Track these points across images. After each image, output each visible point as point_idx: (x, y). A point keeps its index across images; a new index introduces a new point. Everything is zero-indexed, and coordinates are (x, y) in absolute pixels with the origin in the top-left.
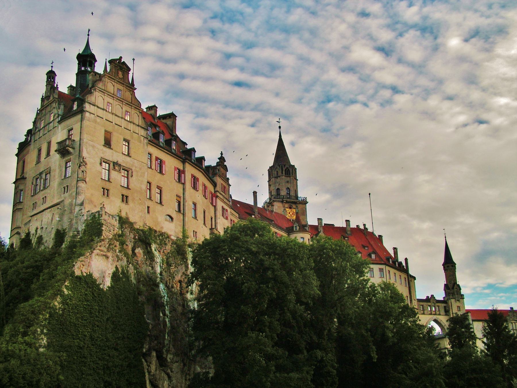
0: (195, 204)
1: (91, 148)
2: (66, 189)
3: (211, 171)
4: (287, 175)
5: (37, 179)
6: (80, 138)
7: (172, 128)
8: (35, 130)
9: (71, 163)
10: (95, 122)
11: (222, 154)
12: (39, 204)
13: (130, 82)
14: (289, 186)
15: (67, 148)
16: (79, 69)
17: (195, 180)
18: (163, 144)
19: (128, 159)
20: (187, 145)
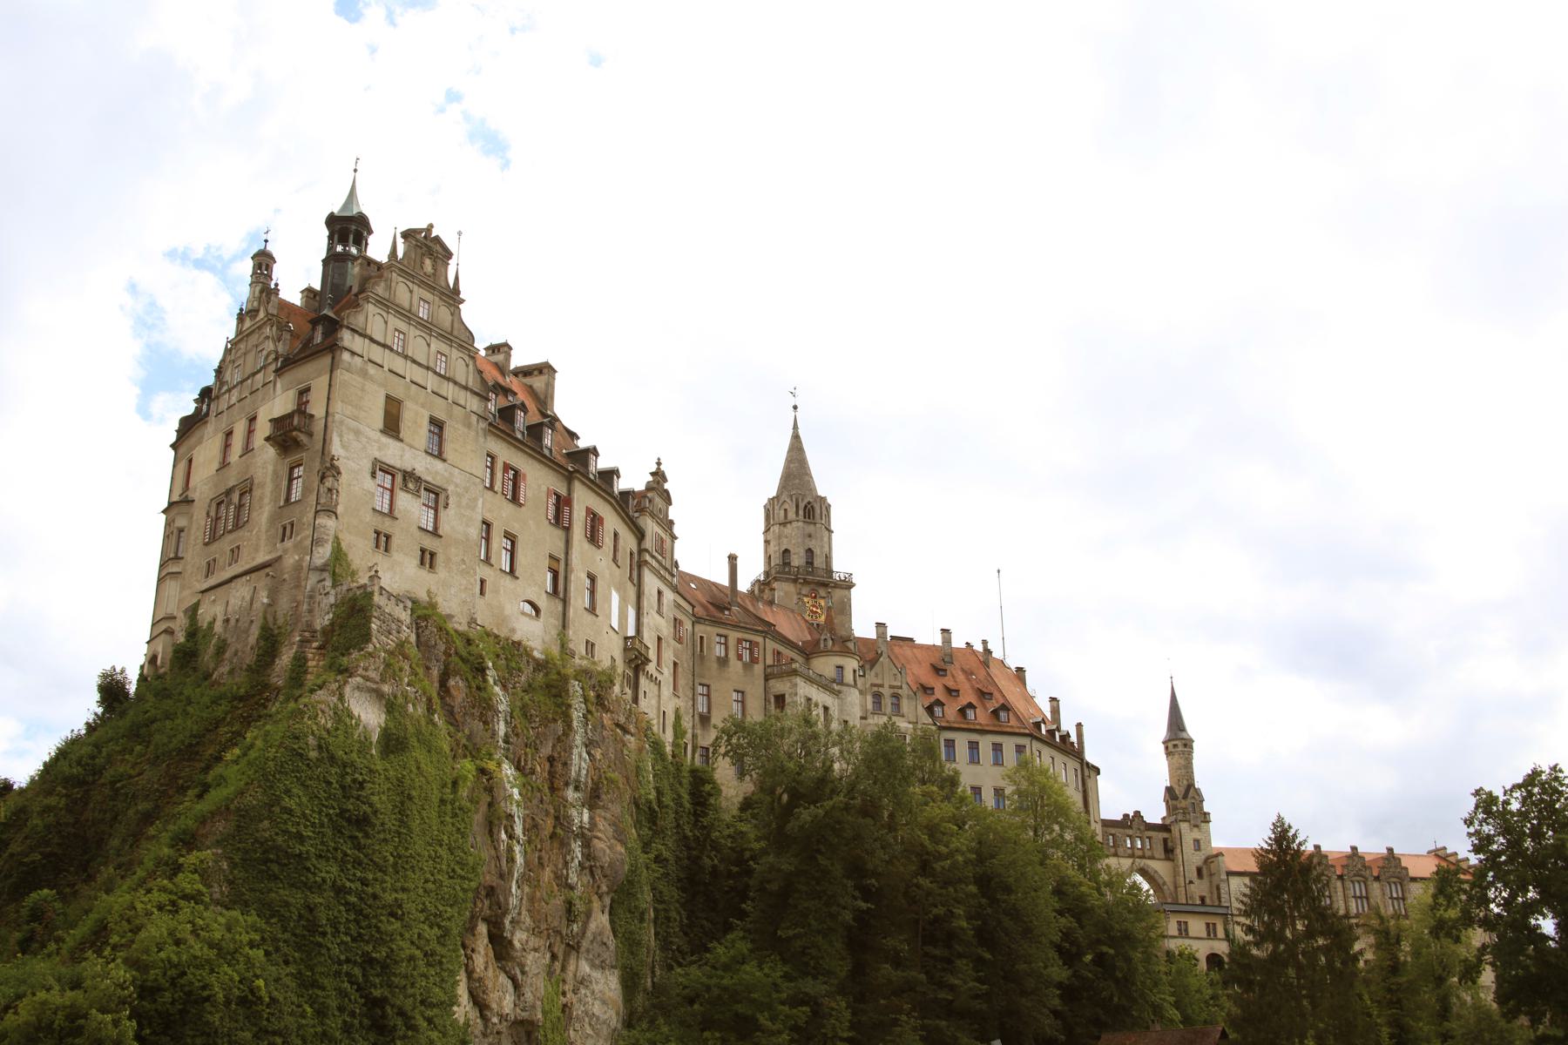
0: (592, 578)
1: (351, 436)
2: (286, 532)
3: (632, 503)
4: (807, 520)
5: (219, 504)
6: (327, 412)
7: (546, 397)
8: (220, 389)
9: (301, 468)
10: (364, 373)
11: (659, 464)
12: (221, 564)
13: (451, 286)
14: (812, 544)
15: (294, 433)
16: (331, 248)
17: (595, 521)
18: (523, 433)
19: (439, 465)
20: (578, 438)
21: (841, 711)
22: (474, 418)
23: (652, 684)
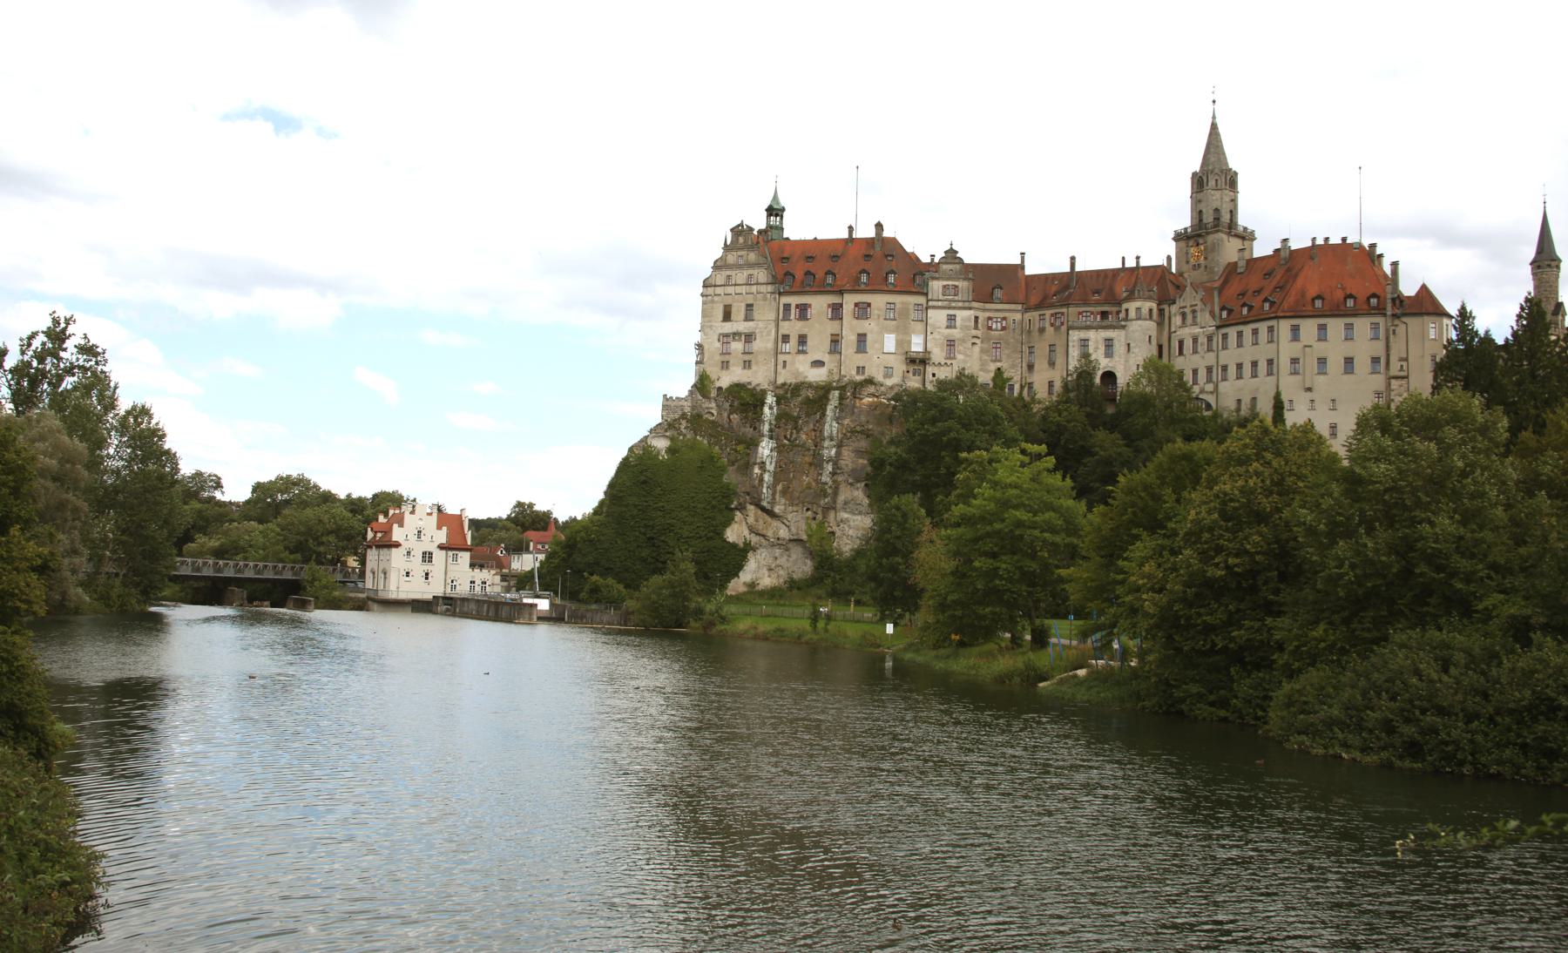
10: (713, 302)
14: (1202, 206)
19: (751, 323)
21: (1126, 339)
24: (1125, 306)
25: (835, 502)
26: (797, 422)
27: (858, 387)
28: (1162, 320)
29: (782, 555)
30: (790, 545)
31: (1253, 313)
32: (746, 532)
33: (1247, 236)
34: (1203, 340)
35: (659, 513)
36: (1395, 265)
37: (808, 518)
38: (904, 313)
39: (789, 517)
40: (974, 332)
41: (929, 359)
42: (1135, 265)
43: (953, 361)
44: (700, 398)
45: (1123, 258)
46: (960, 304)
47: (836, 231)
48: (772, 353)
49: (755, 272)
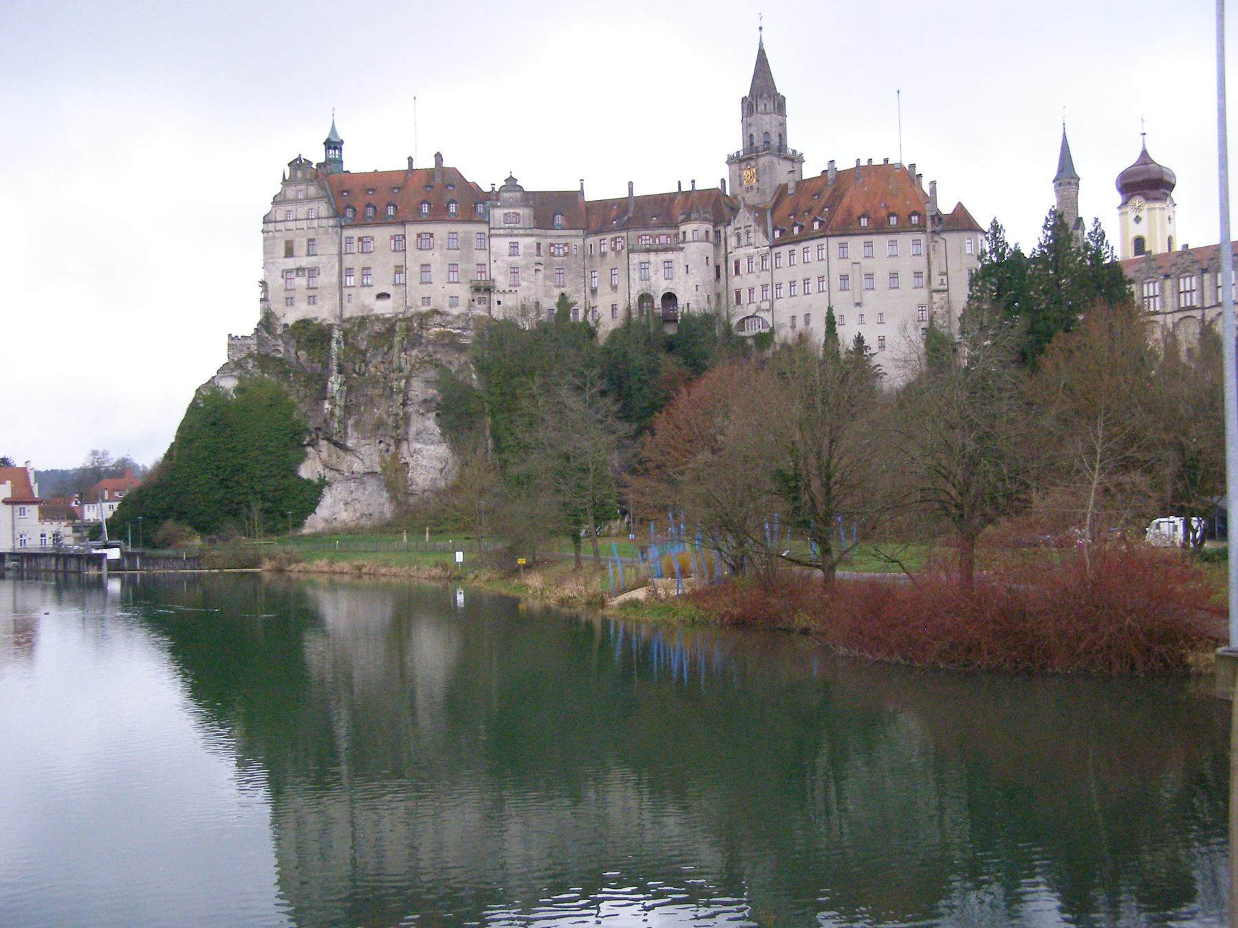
1: (271, 266)
10: (274, 238)
14: (753, 130)
19: (314, 258)
21: (684, 260)
22: (330, 229)
23: (507, 295)
24: (682, 228)
25: (407, 433)
26: (365, 355)
27: (424, 318)
28: (718, 240)
29: (357, 489)
30: (365, 478)
31: (804, 231)
32: (320, 468)
33: (796, 160)
34: (757, 259)
35: (231, 454)
36: (933, 183)
37: (381, 451)
38: (467, 243)
39: (362, 450)
40: (538, 259)
41: (494, 287)
42: (690, 189)
43: (517, 289)
44: (267, 335)
45: (679, 182)
46: (522, 232)
47: (395, 163)
48: (337, 287)
49: (314, 205)
